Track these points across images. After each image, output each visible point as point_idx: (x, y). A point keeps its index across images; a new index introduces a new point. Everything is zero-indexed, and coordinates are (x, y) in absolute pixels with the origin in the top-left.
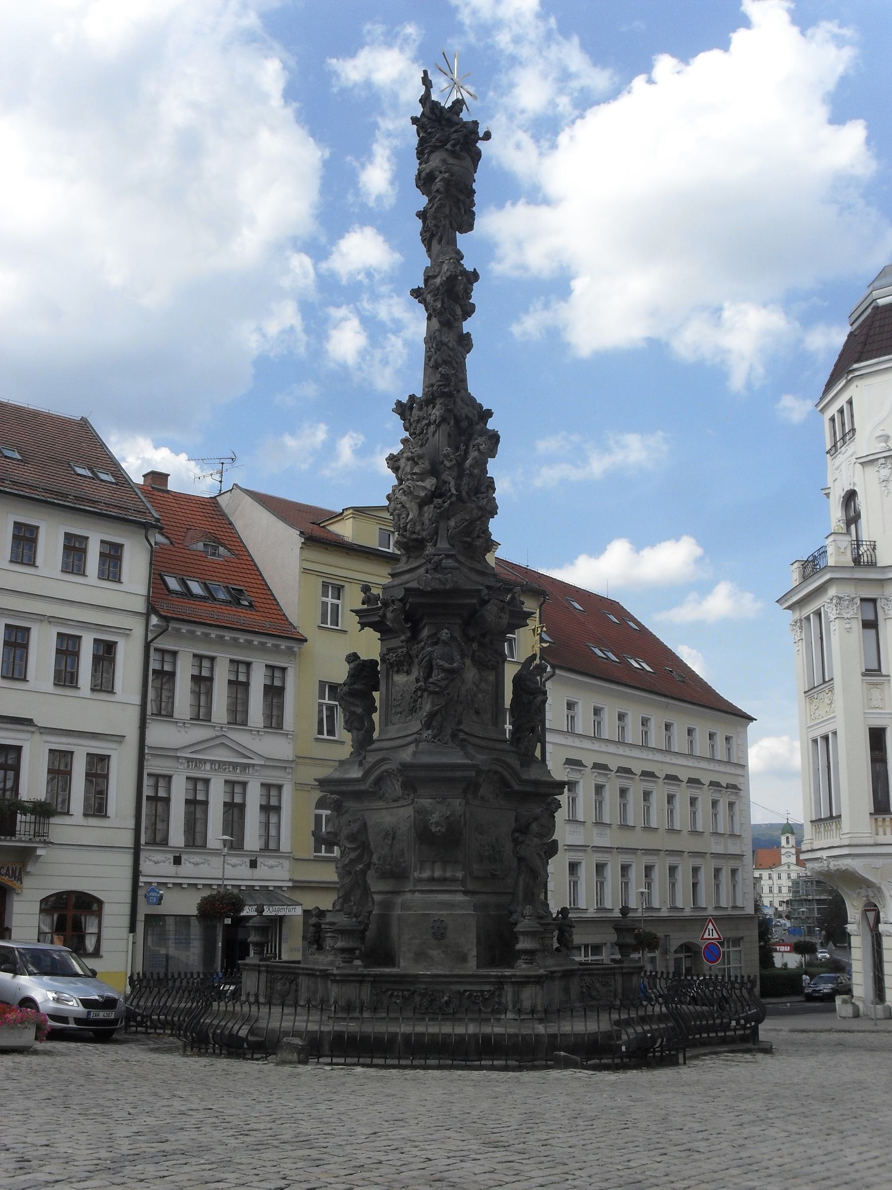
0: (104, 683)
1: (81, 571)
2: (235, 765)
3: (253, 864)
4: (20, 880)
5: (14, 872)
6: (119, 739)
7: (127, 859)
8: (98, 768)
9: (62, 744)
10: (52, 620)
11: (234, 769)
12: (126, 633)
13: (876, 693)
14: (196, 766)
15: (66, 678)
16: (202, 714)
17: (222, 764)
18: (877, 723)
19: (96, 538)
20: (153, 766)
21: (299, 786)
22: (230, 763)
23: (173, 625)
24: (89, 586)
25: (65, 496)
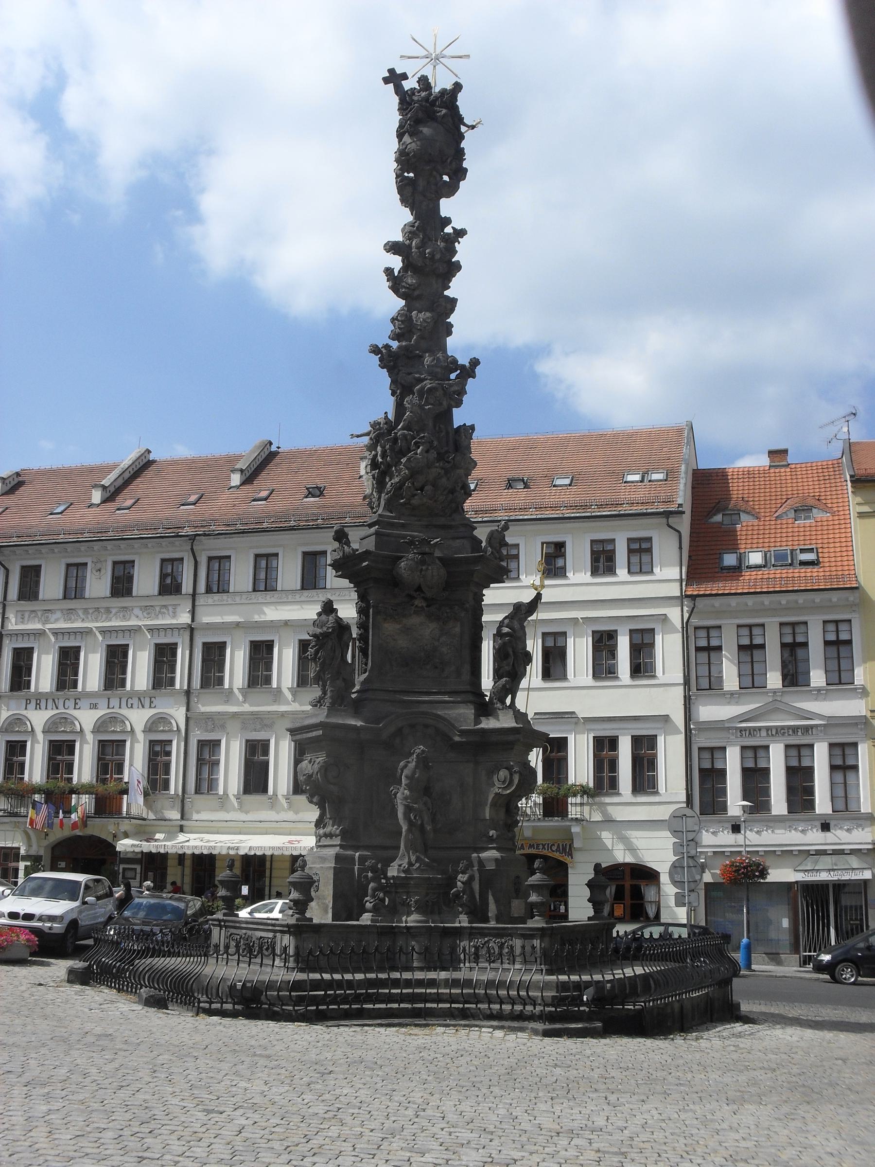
0: (641, 667)
2: (795, 729)
4: (570, 854)
5: (564, 849)
9: (606, 731)
11: (794, 732)
14: (750, 733)
15: (603, 668)
16: (752, 682)
17: (780, 731)
20: (702, 740)
25: (585, 507)
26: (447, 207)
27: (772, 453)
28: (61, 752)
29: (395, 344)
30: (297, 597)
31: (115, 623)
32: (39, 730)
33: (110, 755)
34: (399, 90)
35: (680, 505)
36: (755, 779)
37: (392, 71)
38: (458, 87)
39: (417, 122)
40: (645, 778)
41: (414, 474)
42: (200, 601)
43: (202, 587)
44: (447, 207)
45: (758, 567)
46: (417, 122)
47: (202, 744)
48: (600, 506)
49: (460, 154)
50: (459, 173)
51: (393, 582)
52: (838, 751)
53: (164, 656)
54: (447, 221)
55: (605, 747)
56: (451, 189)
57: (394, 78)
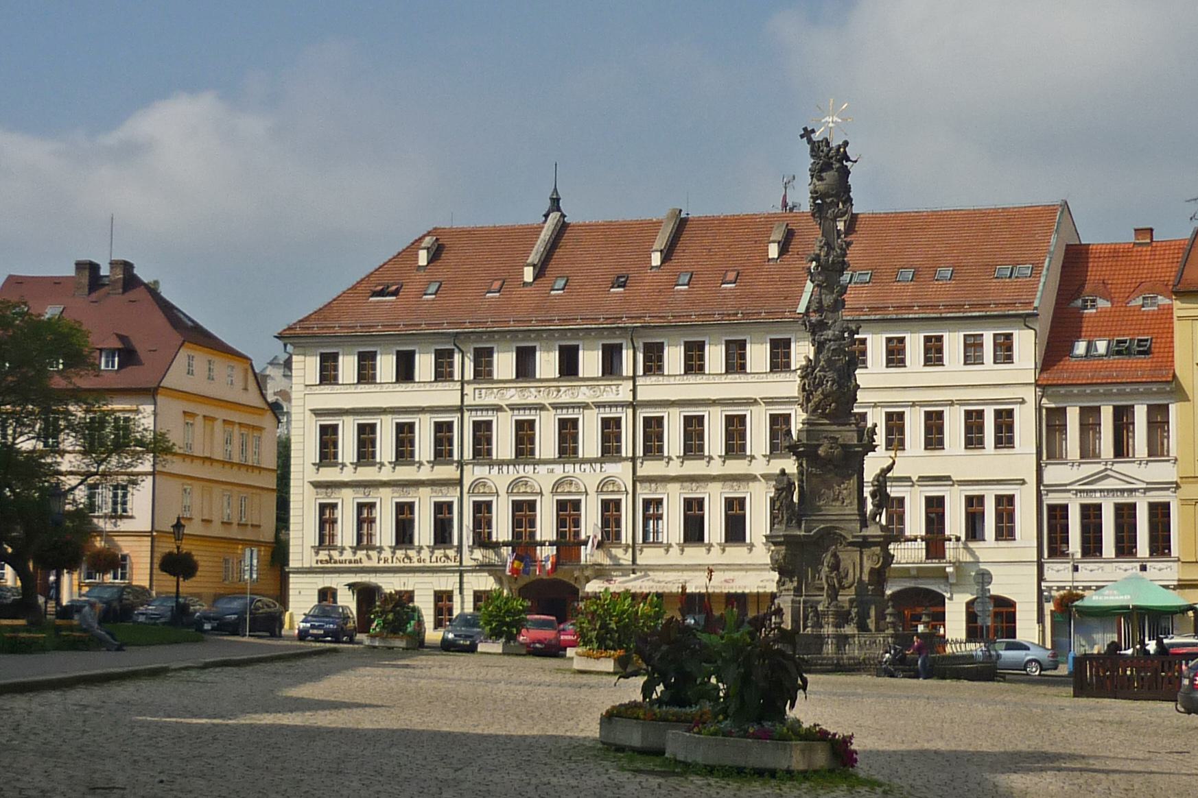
1: (979, 360)
6: (1023, 482)
7: (1034, 569)
8: (1006, 505)
9: (974, 491)
10: (962, 403)
16: (1088, 452)
22: (1117, 490)
23: (1050, 391)
24: (989, 370)
28: (524, 512)
30: (723, 379)
31: (565, 398)
33: (568, 511)
34: (810, 141)
35: (1036, 308)
37: (805, 129)
38: (846, 144)
39: (822, 170)
40: (1005, 531)
41: (826, 396)
42: (640, 381)
46: (822, 170)
47: (647, 503)
49: (848, 189)
53: (610, 429)
55: (974, 506)
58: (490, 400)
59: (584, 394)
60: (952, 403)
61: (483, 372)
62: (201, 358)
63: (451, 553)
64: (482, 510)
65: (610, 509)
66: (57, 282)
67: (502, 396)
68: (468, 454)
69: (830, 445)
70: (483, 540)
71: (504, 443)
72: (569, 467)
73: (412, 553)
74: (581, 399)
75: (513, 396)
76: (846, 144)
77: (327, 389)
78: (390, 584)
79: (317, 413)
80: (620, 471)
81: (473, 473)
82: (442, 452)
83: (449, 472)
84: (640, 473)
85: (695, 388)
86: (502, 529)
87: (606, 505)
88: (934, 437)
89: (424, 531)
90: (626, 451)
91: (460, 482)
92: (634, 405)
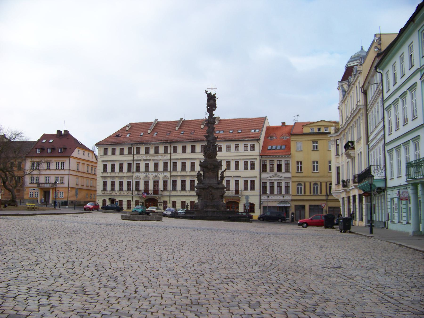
2: (279, 179)
3: (283, 197)
6: (256, 177)
7: (258, 197)
8: (253, 182)
10: (243, 159)
12: (256, 159)
13: (338, 159)
15: (246, 168)
17: (276, 180)
18: (338, 166)
19: (249, 144)
20: (263, 181)
21: (293, 182)
23: (263, 157)
24: (249, 152)
26: (214, 112)
27: (282, 123)
28: (146, 183)
29: (207, 135)
31: (155, 158)
32: (142, 178)
33: (156, 183)
36: (272, 187)
38: (215, 94)
40: (253, 188)
42: (172, 154)
43: (172, 152)
44: (214, 112)
45: (274, 149)
47: (173, 181)
48: (246, 138)
49: (216, 104)
50: (216, 107)
51: (206, 167)
52: (286, 183)
53: (165, 165)
54: (214, 115)
55: (246, 182)
56: (214, 110)
57: (206, 92)
58: (139, 158)
59: (160, 157)
60: (241, 159)
61: (138, 153)
62: (81, 151)
63: (130, 192)
64: (138, 183)
65: (165, 183)
66: (53, 135)
67: (142, 158)
68: (135, 170)
69: (211, 166)
70: (138, 189)
71: (142, 168)
72: (156, 174)
73: (122, 192)
74: (159, 158)
75: (144, 158)
76: (215, 94)
77: (105, 156)
78: (118, 199)
79: (103, 161)
80: (167, 174)
81: (136, 174)
82: (129, 170)
83: (130, 174)
84: (172, 174)
85: (184, 156)
86: (142, 187)
87: (164, 182)
88: (237, 167)
89: (125, 187)
90: (169, 170)
91: (133, 176)
92: (170, 159)
